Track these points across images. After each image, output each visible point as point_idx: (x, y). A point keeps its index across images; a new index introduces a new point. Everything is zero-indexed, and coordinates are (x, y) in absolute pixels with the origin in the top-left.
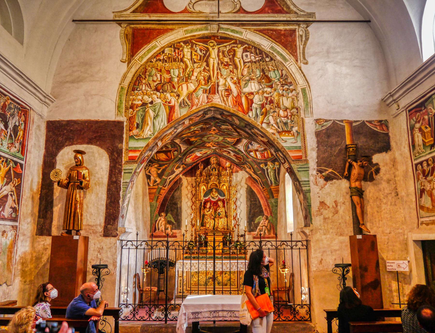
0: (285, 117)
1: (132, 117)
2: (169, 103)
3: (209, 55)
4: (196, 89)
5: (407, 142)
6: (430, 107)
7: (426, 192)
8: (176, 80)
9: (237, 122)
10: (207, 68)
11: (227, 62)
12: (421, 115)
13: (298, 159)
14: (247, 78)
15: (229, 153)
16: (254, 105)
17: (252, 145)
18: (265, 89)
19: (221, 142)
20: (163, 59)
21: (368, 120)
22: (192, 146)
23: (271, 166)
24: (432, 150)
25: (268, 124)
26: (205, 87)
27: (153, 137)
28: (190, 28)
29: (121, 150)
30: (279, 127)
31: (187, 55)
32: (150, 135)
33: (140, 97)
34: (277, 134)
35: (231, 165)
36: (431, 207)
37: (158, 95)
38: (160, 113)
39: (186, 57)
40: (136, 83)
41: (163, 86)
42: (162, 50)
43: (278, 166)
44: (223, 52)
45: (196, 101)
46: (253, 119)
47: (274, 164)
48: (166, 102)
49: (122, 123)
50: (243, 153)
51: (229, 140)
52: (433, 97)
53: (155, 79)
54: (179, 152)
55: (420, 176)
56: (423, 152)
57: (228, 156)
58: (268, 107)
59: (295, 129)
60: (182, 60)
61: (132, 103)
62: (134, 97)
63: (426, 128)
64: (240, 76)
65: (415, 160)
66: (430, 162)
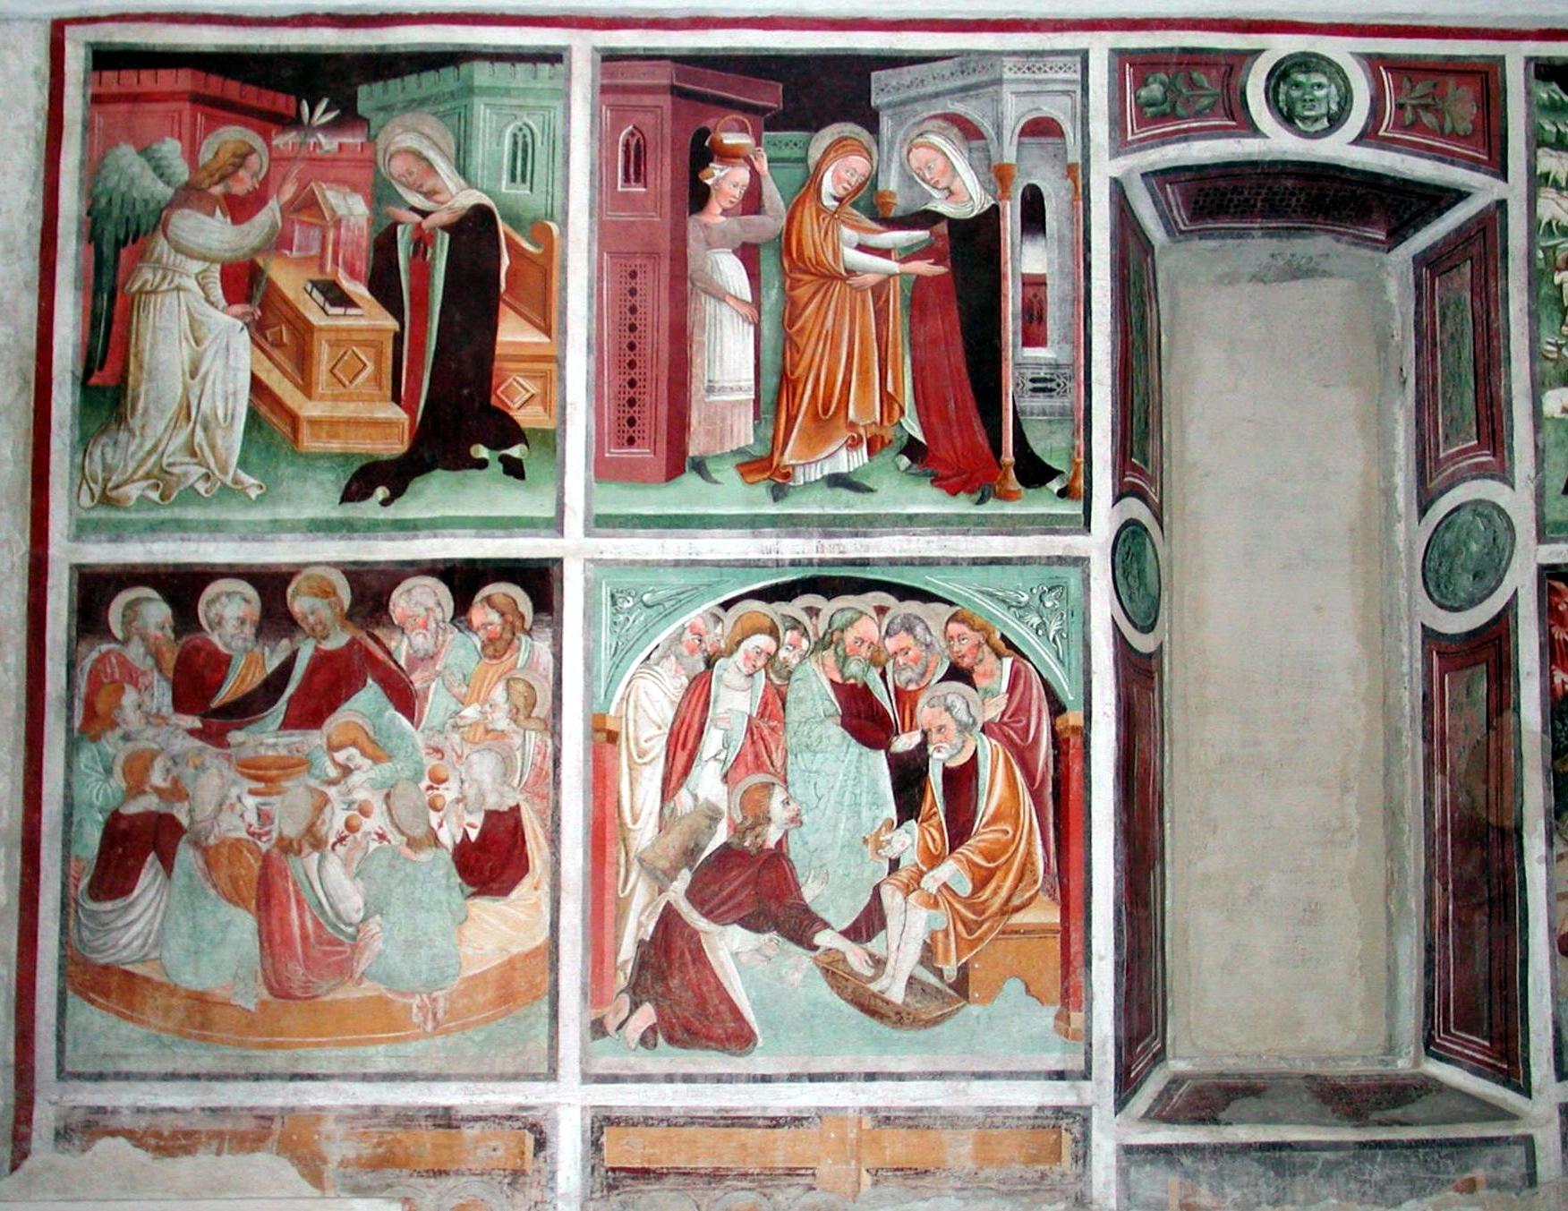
6: (410, 141)
7: (186, 856)
12: (277, 159)
24: (370, 509)
36: (251, 996)
52: (482, 73)
55: (129, 697)
65: (82, 530)
66: (301, 603)
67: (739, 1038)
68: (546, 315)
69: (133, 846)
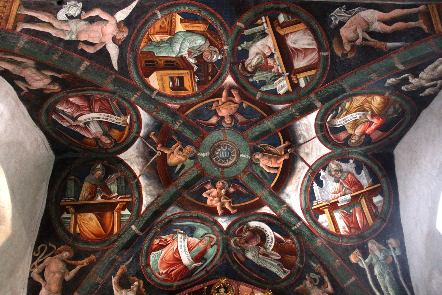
17: (320, 184)
19: (245, 178)
22: (172, 189)
23: (377, 253)
43: (398, 252)
47: (386, 245)
50: (299, 219)
54: (135, 209)
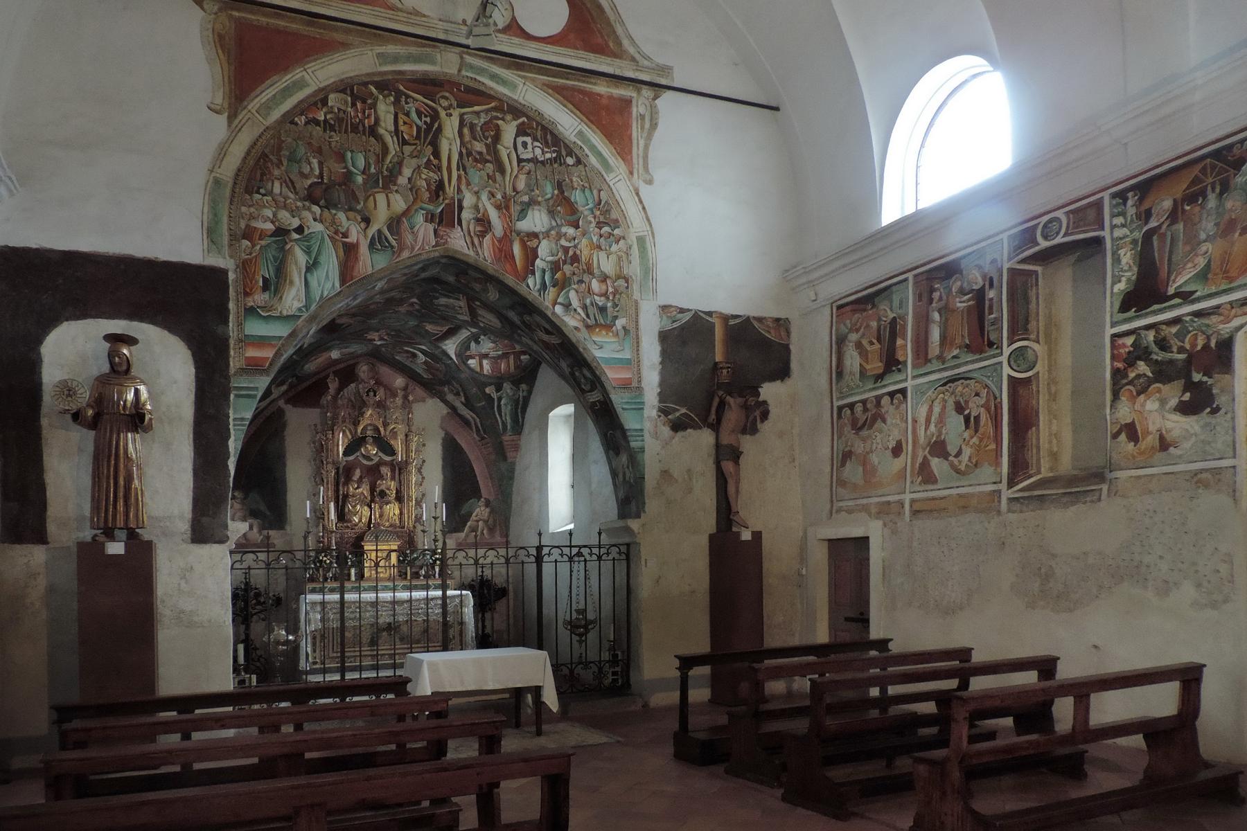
0: (601, 295)
1: (251, 260)
2: (345, 235)
3: (440, 129)
4: (408, 209)
5: (827, 365)
8: (360, 179)
9: (493, 295)
10: (435, 162)
11: (480, 153)
13: (625, 385)
14: (526, 198)
15: (414, 355)
16: (538, 262)
18: (564, 229)
20: (325, 121)
21: (756, 315)
25: (567, 306)
26: (431, 207)
27: (305, 315)
28: (391, 49)
29: (225, 342)
30: (588, 316)
31: (387, 122)
32: (300, 309)
33: (268, 213)
34: (583, 329)
35: (407, 386)
37: (313, 213)
38: (322, 259)
39: (383, 124)
40: (254, 176)
41: (326, 190)
42: (321, 96)
44: (472, 127)
45: (409, 239)
46: (537, 294)
48: (336, 232)
49: (224, 272)
51: (429, 327)
53: (306, 170)
56: (858, 386)
57: (408, 363)
58: (567, 269)
59: (620, 323)
60: (373, 131)
61: (247, 226)
62: (252, 210)
63: (871, 343)
64: (509, 191)
67: (935, 481)
68: (904, 338)
69: (847, 456)
